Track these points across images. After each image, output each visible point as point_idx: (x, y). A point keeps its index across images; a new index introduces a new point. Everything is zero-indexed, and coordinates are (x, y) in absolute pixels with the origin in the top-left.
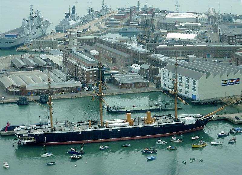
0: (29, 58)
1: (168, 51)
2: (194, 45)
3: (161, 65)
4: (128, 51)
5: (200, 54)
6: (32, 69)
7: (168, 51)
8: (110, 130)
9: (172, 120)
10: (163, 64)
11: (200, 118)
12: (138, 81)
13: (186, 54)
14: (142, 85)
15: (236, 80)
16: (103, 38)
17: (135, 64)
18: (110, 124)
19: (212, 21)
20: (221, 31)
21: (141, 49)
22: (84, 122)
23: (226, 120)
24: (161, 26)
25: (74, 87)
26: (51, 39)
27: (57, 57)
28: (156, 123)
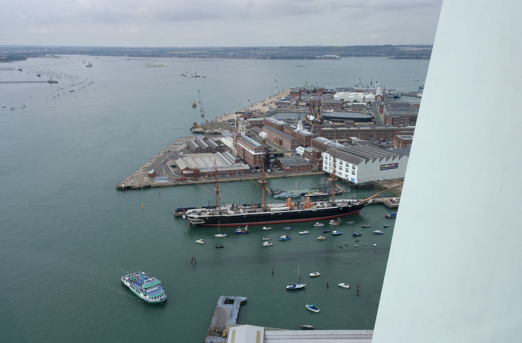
0: (203, 140)
1: (332, 134)
2: (358, 128)
3: (325, 148)
4: (294, 134)
5: (363, 136)
6: (206, 151)
7: (332, 134)
8: (272, 213)
9: (330, 204)
10: (326, 147)
11: (356, 202)
12: (302, 164)
13: (349, 136)
14: (306, 168)
15: (395, 165)
16: (272, 120)
17: (300, 147)
18: (272, 209)
19: (379, 100)
20: (386, 112)
21: (306, 132)
22: (249, 205)
23: (381, 204)
24: (328, 106)
25: (242, 170)
26: (224, 121)
27: (228, 139)
28: (315, 207)
